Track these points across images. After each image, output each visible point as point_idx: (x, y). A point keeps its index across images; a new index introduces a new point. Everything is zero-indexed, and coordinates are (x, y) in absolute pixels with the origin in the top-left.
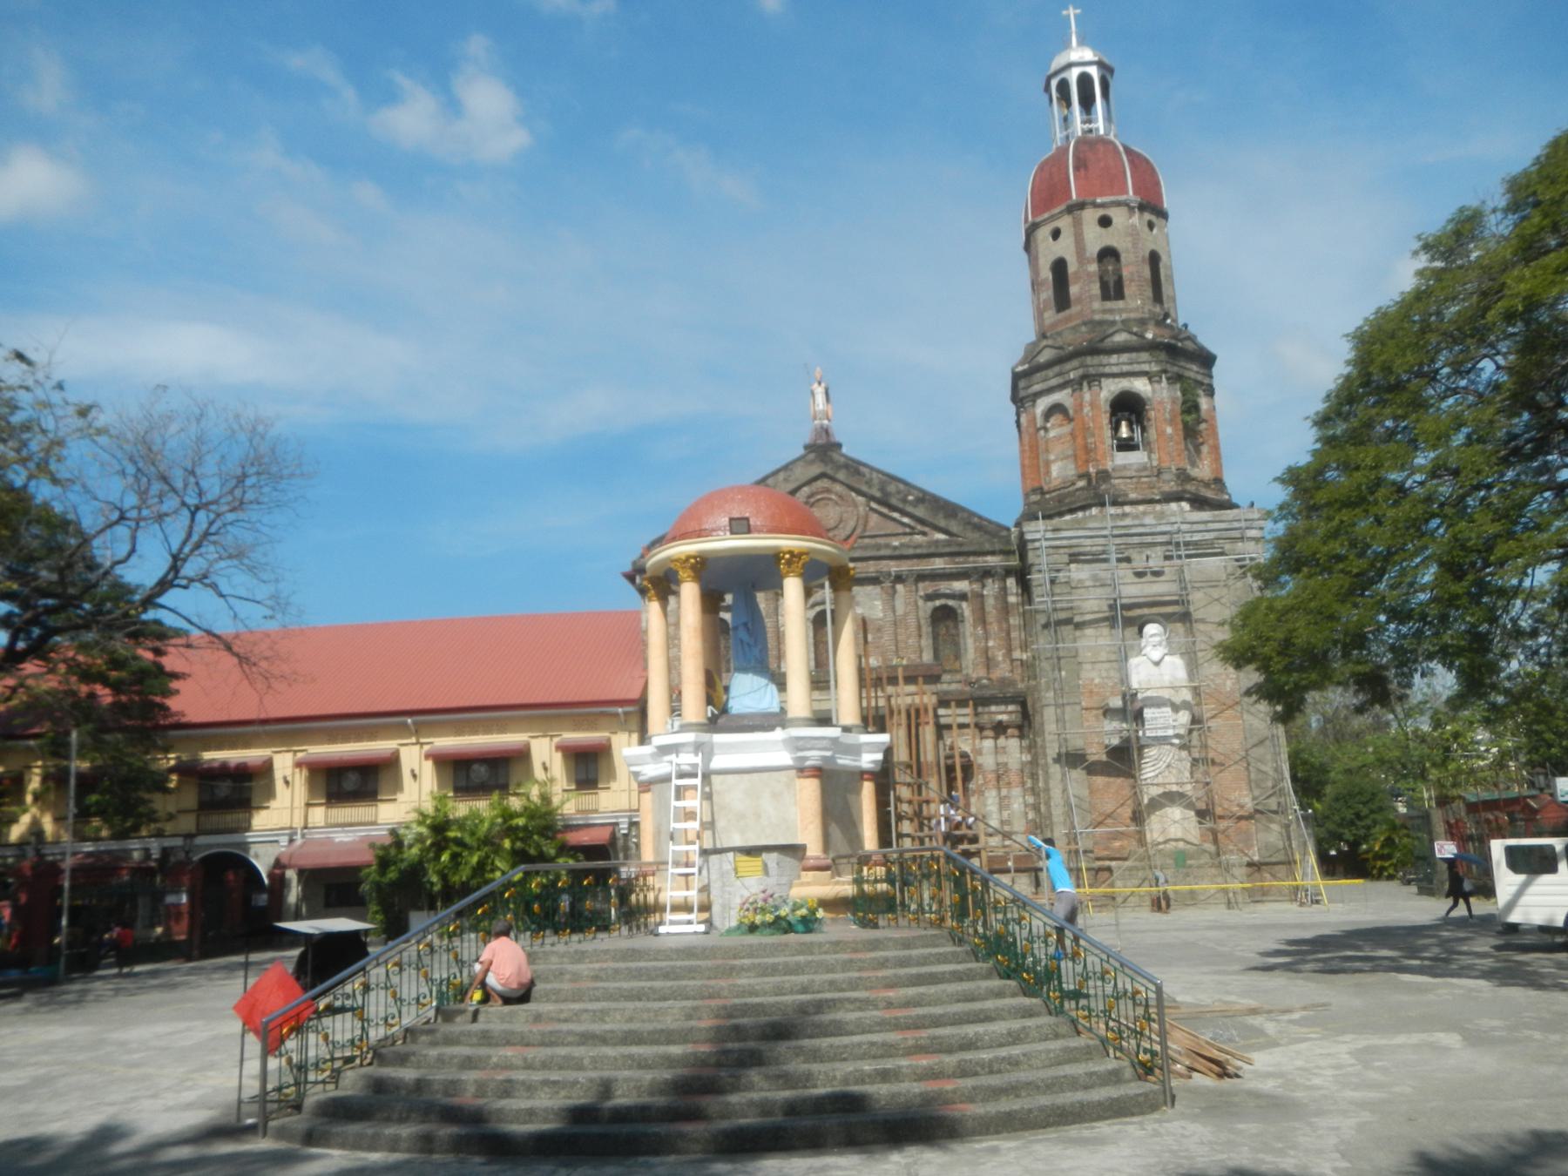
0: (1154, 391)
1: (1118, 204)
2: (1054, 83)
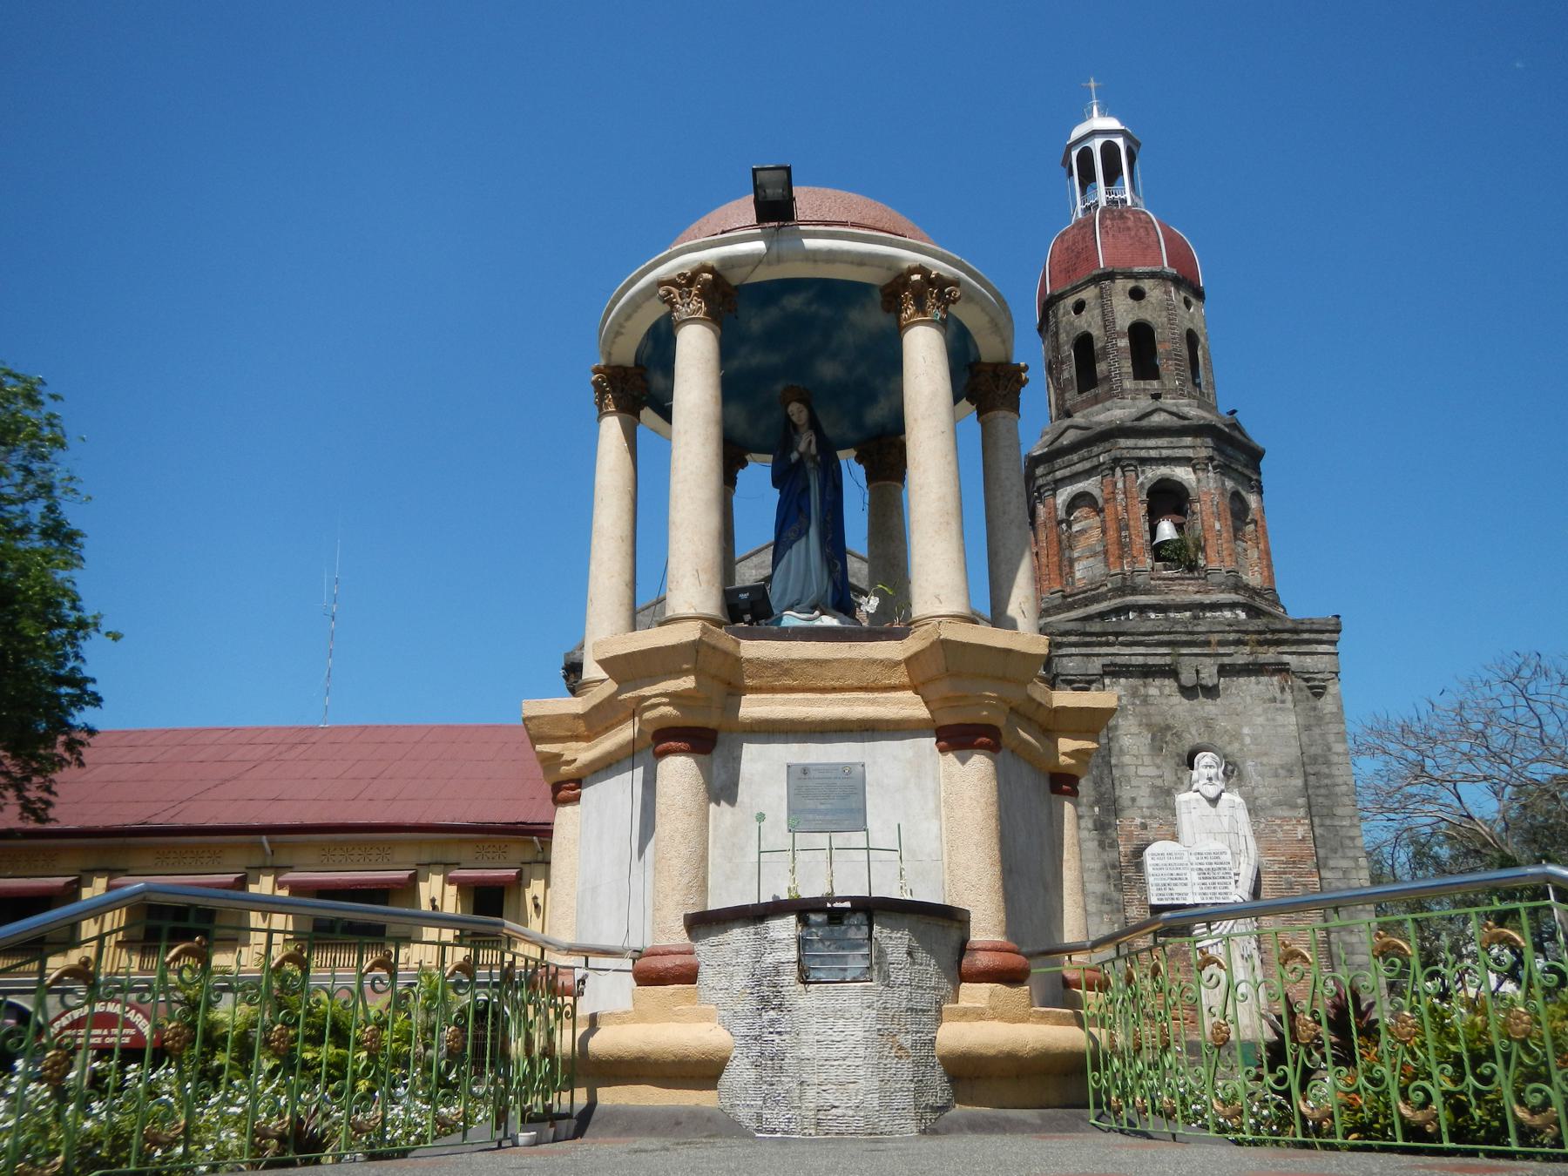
0: (1199, 481)
1: (1152, 275)
2: (1074, 154)
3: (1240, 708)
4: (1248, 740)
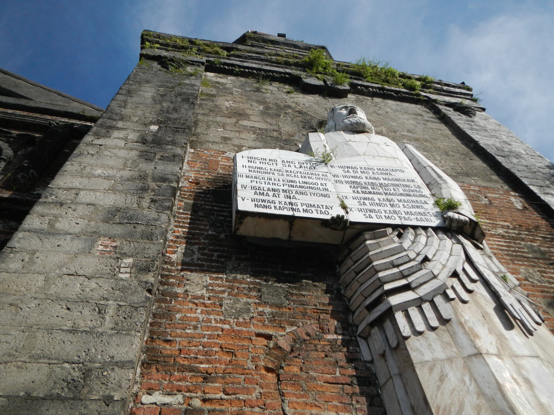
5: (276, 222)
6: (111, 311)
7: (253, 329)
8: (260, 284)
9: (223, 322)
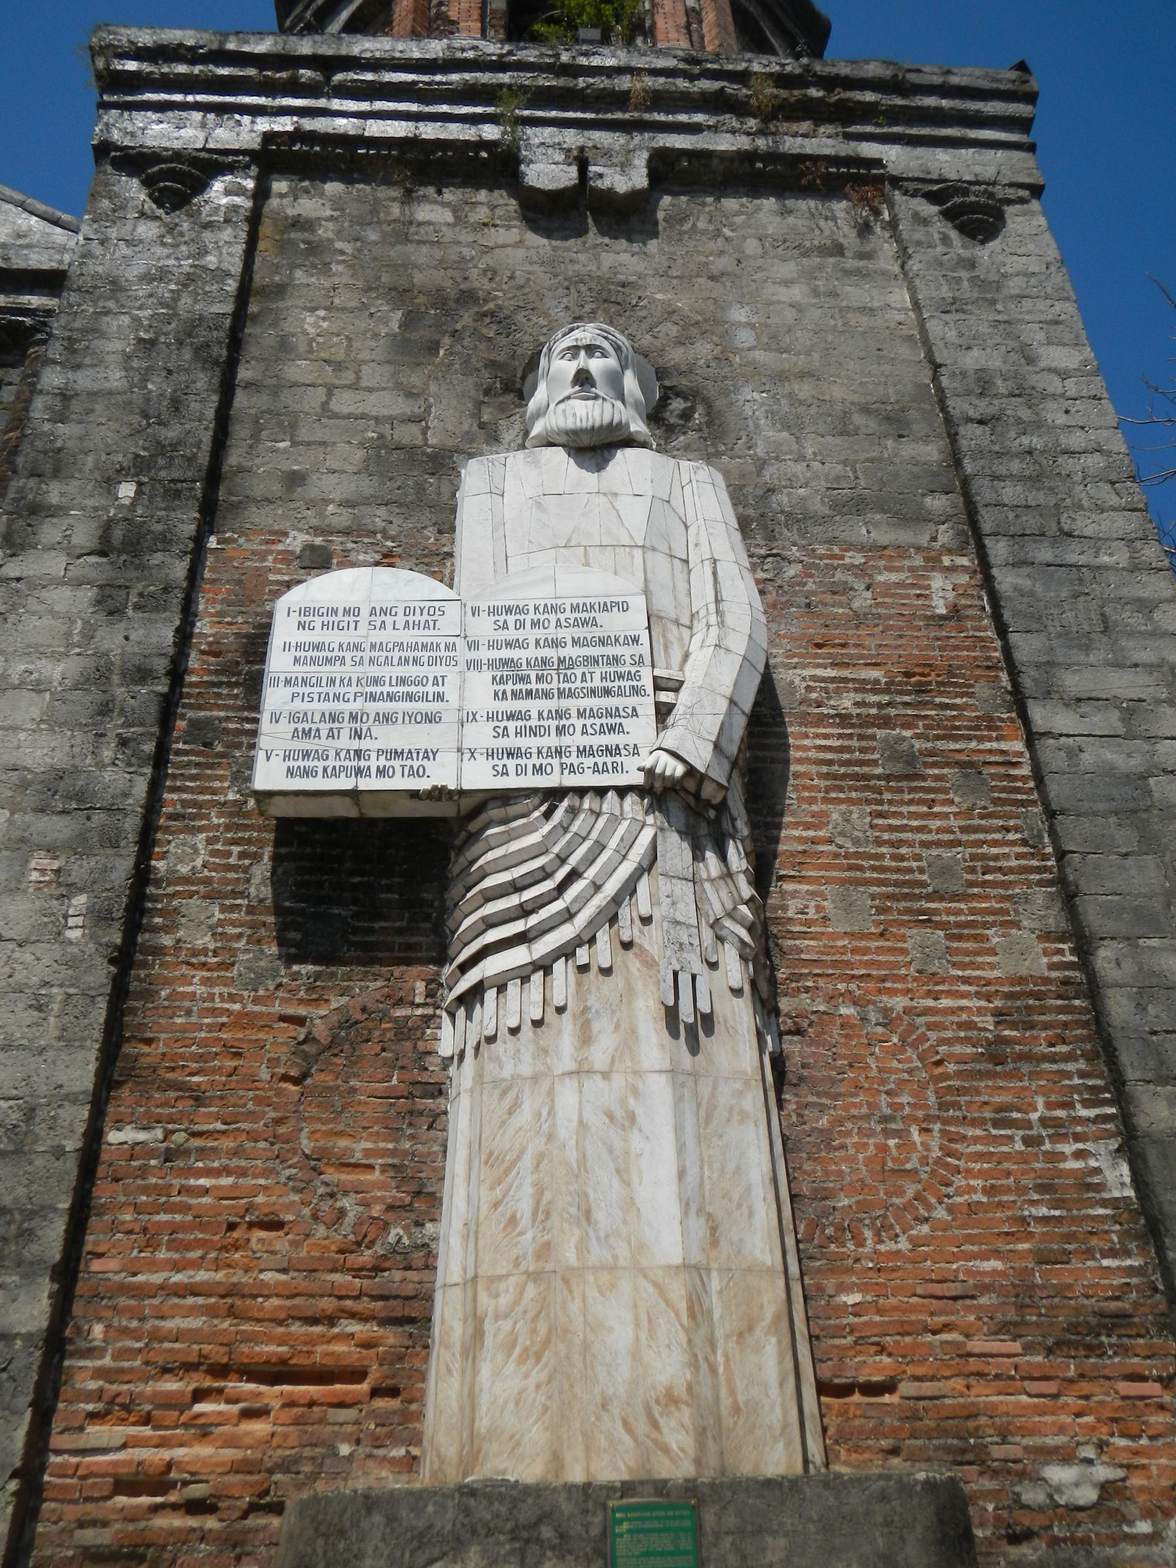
3: (721, 264)
4: (745, 338)
5: (329, 800)
6: (56, 1007)
7: (277, 1008)
8: (301, 913)
9: (232, 998)
